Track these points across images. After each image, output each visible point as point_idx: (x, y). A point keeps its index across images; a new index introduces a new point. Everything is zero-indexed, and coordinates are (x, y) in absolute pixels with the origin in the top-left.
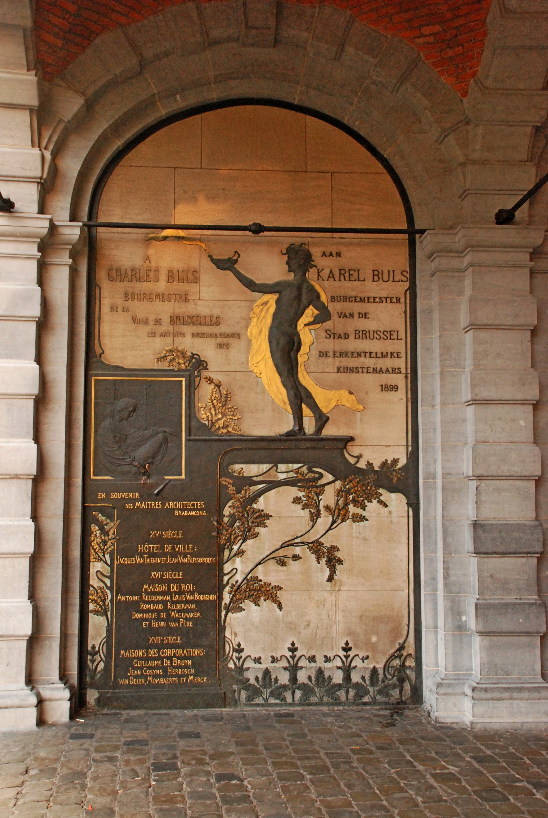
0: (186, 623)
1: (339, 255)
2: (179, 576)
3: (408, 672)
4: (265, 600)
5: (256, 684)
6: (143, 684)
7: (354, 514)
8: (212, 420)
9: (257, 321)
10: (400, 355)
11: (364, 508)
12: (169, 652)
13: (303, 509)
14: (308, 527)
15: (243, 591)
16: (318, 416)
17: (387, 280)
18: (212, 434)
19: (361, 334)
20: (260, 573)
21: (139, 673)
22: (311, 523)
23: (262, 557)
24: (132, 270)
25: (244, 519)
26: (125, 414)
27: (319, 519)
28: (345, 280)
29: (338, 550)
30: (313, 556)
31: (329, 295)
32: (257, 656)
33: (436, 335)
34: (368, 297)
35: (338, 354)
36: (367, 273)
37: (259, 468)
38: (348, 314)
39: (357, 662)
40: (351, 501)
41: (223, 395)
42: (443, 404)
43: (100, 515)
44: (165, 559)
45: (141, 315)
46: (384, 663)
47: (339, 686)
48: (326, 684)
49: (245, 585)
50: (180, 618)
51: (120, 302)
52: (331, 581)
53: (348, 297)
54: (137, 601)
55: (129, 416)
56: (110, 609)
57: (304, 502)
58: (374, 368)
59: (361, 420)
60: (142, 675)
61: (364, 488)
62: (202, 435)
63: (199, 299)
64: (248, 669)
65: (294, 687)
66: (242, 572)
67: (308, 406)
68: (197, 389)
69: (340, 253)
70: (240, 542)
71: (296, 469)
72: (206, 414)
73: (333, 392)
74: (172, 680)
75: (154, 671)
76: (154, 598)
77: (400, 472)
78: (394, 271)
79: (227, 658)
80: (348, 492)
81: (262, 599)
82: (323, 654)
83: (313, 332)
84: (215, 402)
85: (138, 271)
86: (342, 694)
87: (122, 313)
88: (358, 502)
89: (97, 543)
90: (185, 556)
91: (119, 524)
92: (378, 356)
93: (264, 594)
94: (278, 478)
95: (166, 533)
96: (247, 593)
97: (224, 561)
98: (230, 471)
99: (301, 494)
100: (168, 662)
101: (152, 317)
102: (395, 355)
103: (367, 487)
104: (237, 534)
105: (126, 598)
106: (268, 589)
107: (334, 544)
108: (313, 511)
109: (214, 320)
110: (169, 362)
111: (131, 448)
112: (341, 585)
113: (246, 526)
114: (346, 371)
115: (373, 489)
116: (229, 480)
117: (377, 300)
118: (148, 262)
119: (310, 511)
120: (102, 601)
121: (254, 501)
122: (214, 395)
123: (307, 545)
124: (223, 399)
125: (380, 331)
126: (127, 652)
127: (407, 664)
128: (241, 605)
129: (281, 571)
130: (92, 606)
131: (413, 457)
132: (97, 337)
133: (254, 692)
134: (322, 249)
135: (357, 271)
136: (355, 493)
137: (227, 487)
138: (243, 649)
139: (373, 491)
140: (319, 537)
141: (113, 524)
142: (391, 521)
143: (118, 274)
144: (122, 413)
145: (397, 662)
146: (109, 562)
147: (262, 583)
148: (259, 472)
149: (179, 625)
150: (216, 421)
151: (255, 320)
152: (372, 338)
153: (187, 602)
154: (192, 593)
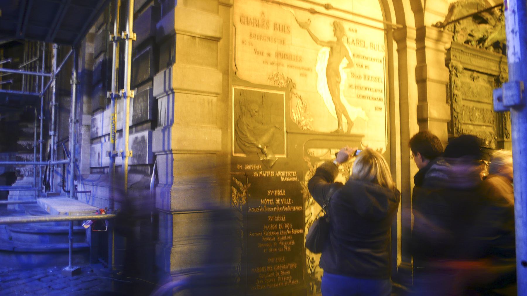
51: (247, 38)
101: (266, 52)
153: (288, 235)
154: (290, 229)
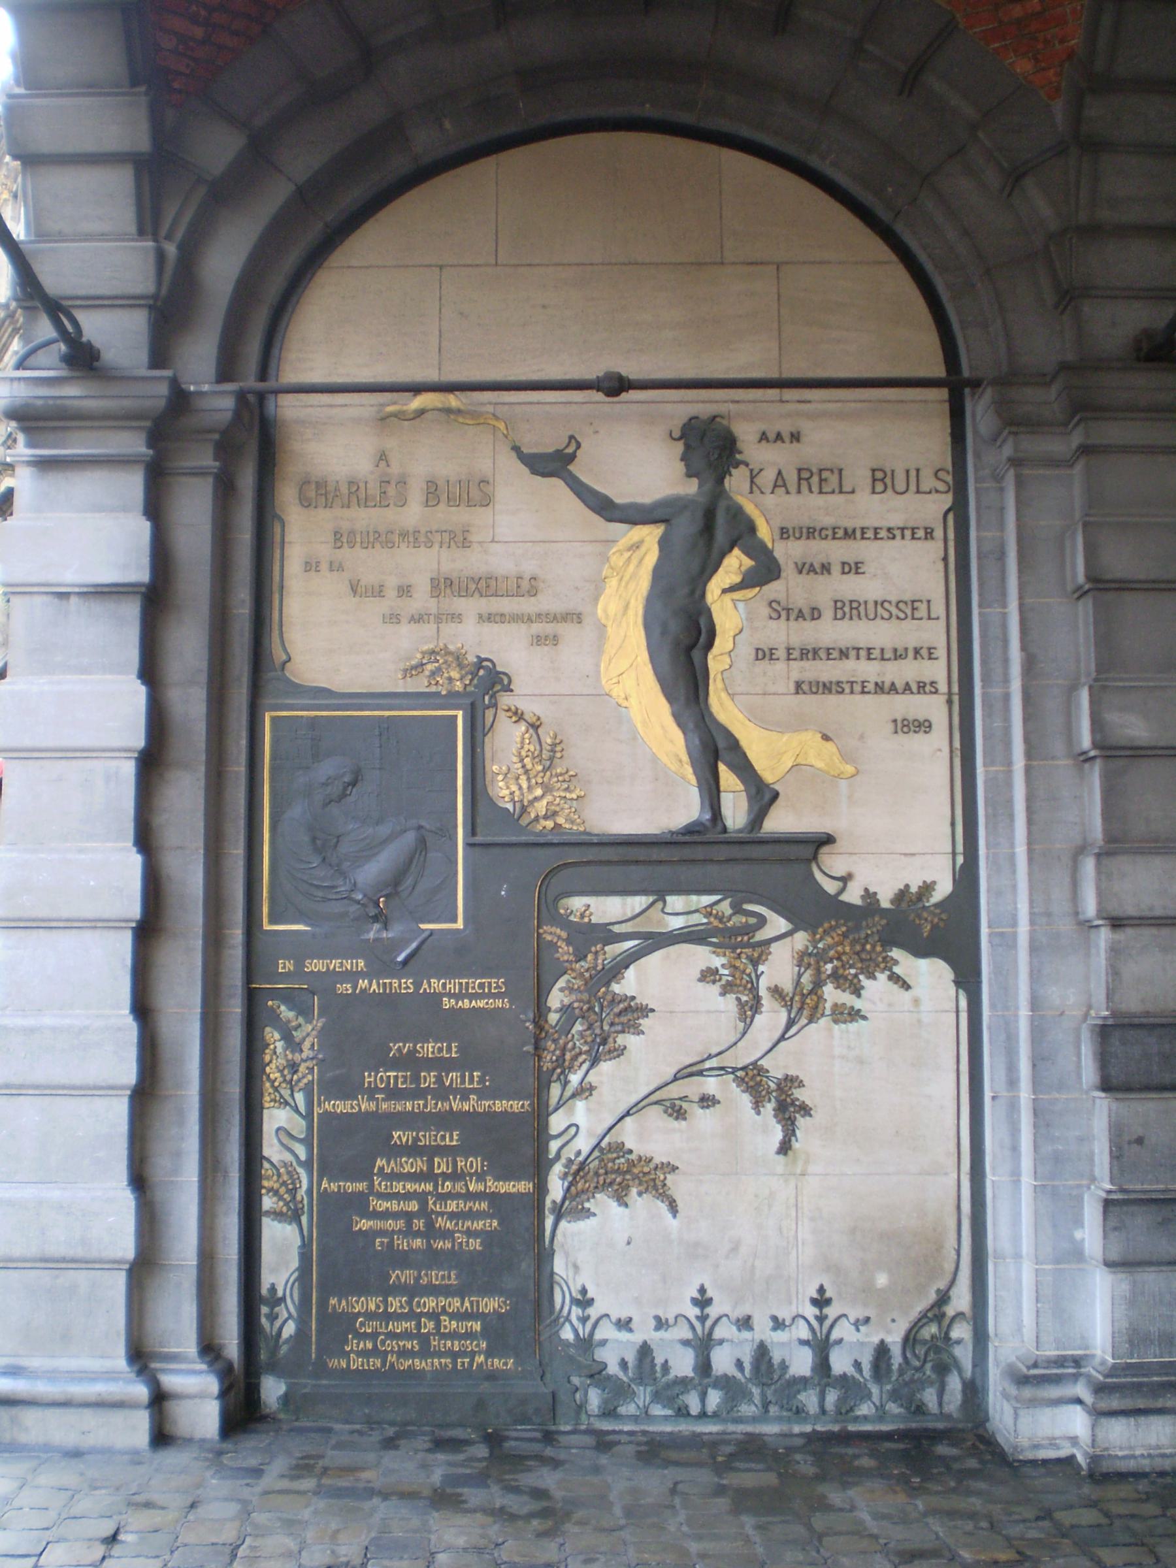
0: (467, 1242)
1: (796, 437)
2: (451, 1139)
3: (958, 1351)
4: (640, 1194)
5: (621, 1375)
6: (377, 1370)
7: (836, 1005)
9: (619, 584)
10: (936, 654)
11: (857, 991)
13: (723, 994)
15: (591, 1173)
16: (753, 791)
17: (904, 489)
18: (523, 830)
19: (847, 609)
20: (630, 1135)
21: (369, 1345)
24: (350, 483)
25: (593, 1017)
26: (335, 789)
28: (811, 491)
29: (801, 1084)
30: (745, 1100)
31: (778, 523)
32: (624, 1316)
34: (863, 529)
35: (796, 654)
36: (858, 476)
37: (624, 904)
38: (817, 567)
39: (843, 1331)
40: (829, 976)
43: (283, 1008)
44: (421, 1102)
45: (369, 578)
47: (803, 1382)
48: (776, 1377)
49: (597, 1162)
50: (454, 1232)
51: (324, 551)
52: (785, 1154)
53: (818, 529)
54: (361, 1193)
55: (344, 795)
56: (306, 1209)
57: (725, 978)
58: (876, 684)
60: (375, 1352)
61: (858, 948)
62: (504, 840)
63: (493, 541)
64: (603, 1343)
65: (706, 1381)
66: (590, 1133)
67: (732, 767)
68: (490, 734)
69: (799, 433)
72: (508, 788)
73: (786, 737)
74: (440, 1363)
76: (398, 1187)
77: (938, 911)
78: (918, 470)
79: (558, 1318)
80: (821, 957)
83: (741, 605)
84: (527, 761)
87: (328, 574)
88: (846, 978)
89: (277, 1067)
90: (465, 1096)
91: (322, 1028)
92: (886, 656)
93: (637, 1181)
94: (667, 925)
95: (422, 1048)
96: (601, 1178)
97: (551, 1109)
98: (562, 911)
99: (717, 962)
100: (431, 1325)
101: (392, 582)
102: (924, 652)
103: (864, 946)
104: (577, 1050)
105: (339, 1186)
106: (646, 1170)
107: (792, 1072)
108: (744, 998)
109: (525, 585)
112: (807, 1162)
113: (598, 1031)
114: (814, 689)
115: (879, 949)
116: (558, 931)
119: (738, 999)
120: (288, 1191)
121: (614, 977)
122: (526, 747)
123: (732, 1073)
124: (546, 755)
125: (890, 602)
126: (344, 1303)
127: (955, 1334)
128: (587, 1205)
130: (268, 1202)
131: (966, 878)
132: (275, 626)
133: (618, 1391)
134: (761, 426)
135: (836, 472)
136: (839, 959)
137: (553, 946)
140: (759, 1055)
141: (310, 1027)
142: (919, 1021)
143: (319, 493)
144: (330, 788)
146: (302, 1109)
148: (625, 914)
149: (453, 1246)
150: (531, 802)
151: (613, 582)
152: (872, 616)
153: (470, 1196)
154: (481, 1177)
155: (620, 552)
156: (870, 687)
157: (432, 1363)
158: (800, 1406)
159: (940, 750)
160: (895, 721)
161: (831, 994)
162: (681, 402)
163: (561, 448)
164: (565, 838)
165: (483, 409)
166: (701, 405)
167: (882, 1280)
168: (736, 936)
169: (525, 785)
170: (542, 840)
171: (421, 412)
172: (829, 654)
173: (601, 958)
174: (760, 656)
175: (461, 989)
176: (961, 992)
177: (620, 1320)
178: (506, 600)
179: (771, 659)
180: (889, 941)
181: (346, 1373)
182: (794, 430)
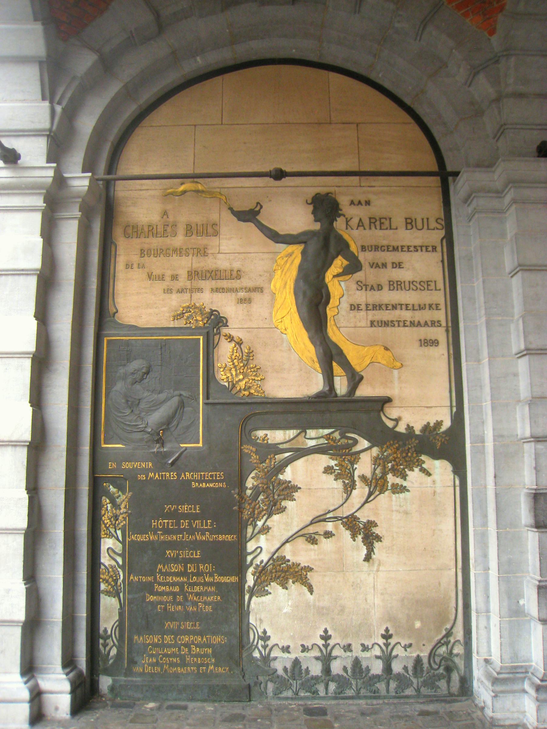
0: (205, 607)
3: (456, 660)
4: (293, 583)
5: (285, 675)
6: (158, 673)
8: (232, 382)
11: (404, 477)
12: (187, 639)
13: (336, 480)
14: (341, 499)
19: (395, 285)
20: (288, 552)
21: (155, 660)
22: (345, 495)
23: (291, 533)
26: (138, 376)
27: (354, 491)
29: (376, 525)
30: (347, 534)
31: (359, 244)
32: (285, 645)
33: (478, 284)
35: (370, 307)
36: (399, 220)
37: (285, 434)
38: (380, 264)
39: (398, 651)
40: (390, 470)
41: (245, 354)
42: (492, 357)
43: (111, 487)
44: (181, 536)
45: (157, 272)
46: (429, 651)
48: (364, 675)
49: (272, 566)
51: (135, 259)
54: (151, 582)
55: (142, 379)
57: (337, 471)
58: (411, 322)
59: (399, 378)
60: (157, 664)
61: (404, 455)
63: (219, 253)
64: (275, 658)
66: (268, 552)
68: (216, 348)
69: (369, 201)
70: (265, 518)
71: (326, 435)
74: (191, 669)
75: (171, 659)
76: (169, 579)
77: (444, 436)
78: (428, 219)
80: (385, 460)
81: (291, 581)
82: (360, 642)
83: (343, 284)
85: (155, 227)
86: (381, 686)
88: (398, 471)
90: (203, 534)
91: (131, 497)
93: (292, 576)
94: (307, 444)
95: (181, 508)
96: (274, 575)
97: (247, 539)
98: (253, 438)
99: (333, 463)
100: (187, 650)
101: (168, 273)
102: (434, 306)
103: (407, 454)
104: (261, 509)
105: (139, 579)
106: (297, 570)
107: (372, 519)
109: (234, 274)
110: (186, 319)
111: (144, 413)
112: (379, 565)
113: (271, 499)
114: (380, 325)
116: (251, 448)
117: (412, 249)
118: (165, 217)
119: (344, 482)
120: (113, 580)
121: (280, 471)
122: (235, 354)
125: (416, 282)
126: (141, 638)
127: (455, 651)
129: (311, 550)
130: (103, 586)
131: (458, 418)
136: (395, 461)
137: (250, 456)
138: (270, 637)
139: (414, 458)
140: (354, 511)
143: (134, 231)
144: (135, 376)
145: (443, 650)
146: (120, 538)
147: (290, 563)
149: (197, 609)
152: (407, 289)
153: (206, 584)
154: (211, 575)
155: (282, 258)
156: (408, 323)
157: (187, 669)
158: (376, 690)
159: (443, 355)
160: (420, 340)
161: (391, 479)
162: (311, 186)
163: (253, 208)
164: (253, 400)
165: (215, 190)
166: (320, 188)
167: (418, 624)
168: (343, 449)
169: (234, 373)
170: (242, 401)
171: (184, 192)
172: (387, 307)
173: (273, 461)
174: (353, 308)
175: (201, 478)
176: (456, 476)
177: (283, 647)
178: (225, 282)
179: (358, 310)
180: (420, 452)
181: (142, 674)
182: (367, 199)
